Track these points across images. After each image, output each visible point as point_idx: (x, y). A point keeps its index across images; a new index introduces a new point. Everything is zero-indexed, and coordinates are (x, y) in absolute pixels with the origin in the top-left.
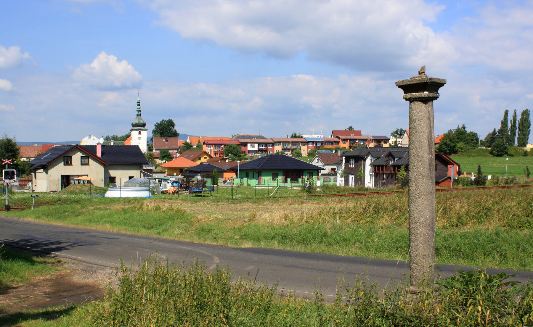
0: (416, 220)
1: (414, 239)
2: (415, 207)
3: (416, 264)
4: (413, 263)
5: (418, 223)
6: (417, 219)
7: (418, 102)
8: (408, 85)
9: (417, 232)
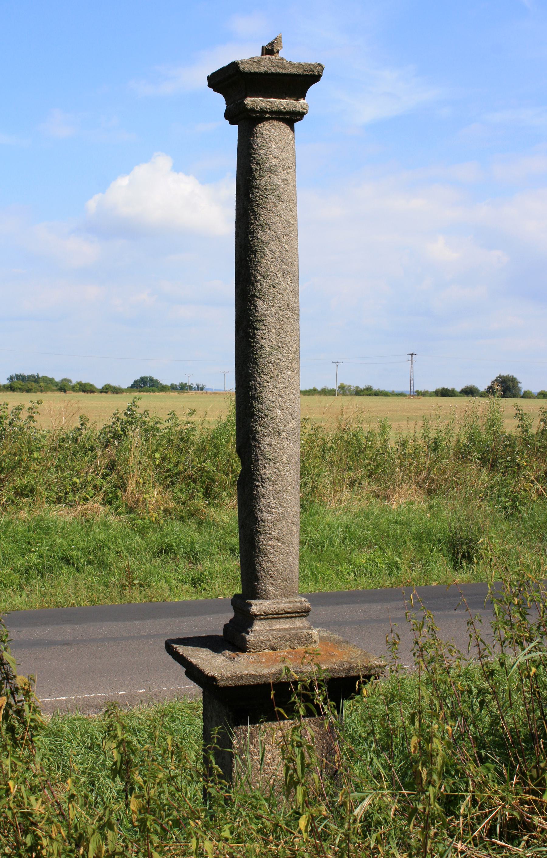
0: (279, 424)
1: (275, 476)
2: (276, 391)
3: (279, 540)
4: (271, 539)
5: (284, 434)
6: (281, 423)
7: (281, 123)
8: (272, 74)
9: (281, 456)
